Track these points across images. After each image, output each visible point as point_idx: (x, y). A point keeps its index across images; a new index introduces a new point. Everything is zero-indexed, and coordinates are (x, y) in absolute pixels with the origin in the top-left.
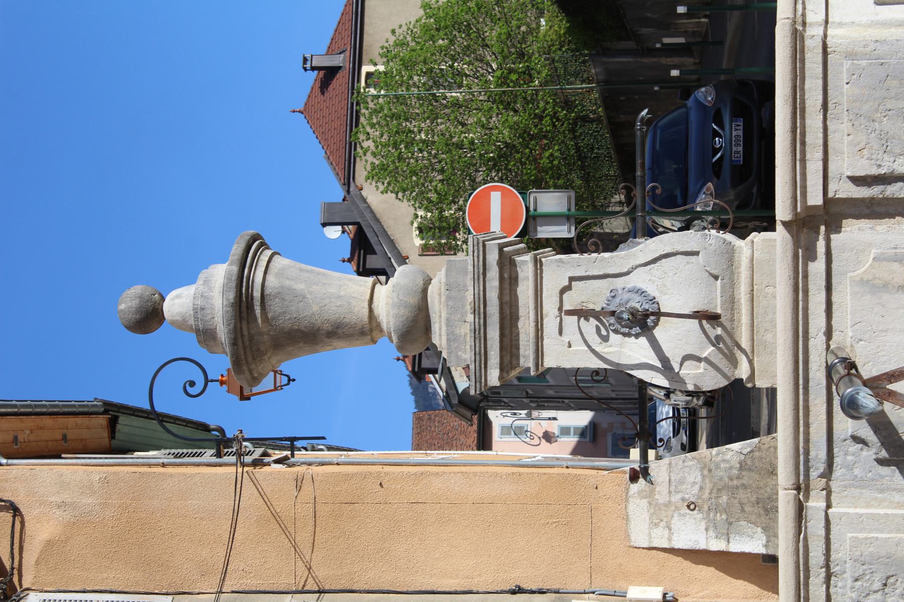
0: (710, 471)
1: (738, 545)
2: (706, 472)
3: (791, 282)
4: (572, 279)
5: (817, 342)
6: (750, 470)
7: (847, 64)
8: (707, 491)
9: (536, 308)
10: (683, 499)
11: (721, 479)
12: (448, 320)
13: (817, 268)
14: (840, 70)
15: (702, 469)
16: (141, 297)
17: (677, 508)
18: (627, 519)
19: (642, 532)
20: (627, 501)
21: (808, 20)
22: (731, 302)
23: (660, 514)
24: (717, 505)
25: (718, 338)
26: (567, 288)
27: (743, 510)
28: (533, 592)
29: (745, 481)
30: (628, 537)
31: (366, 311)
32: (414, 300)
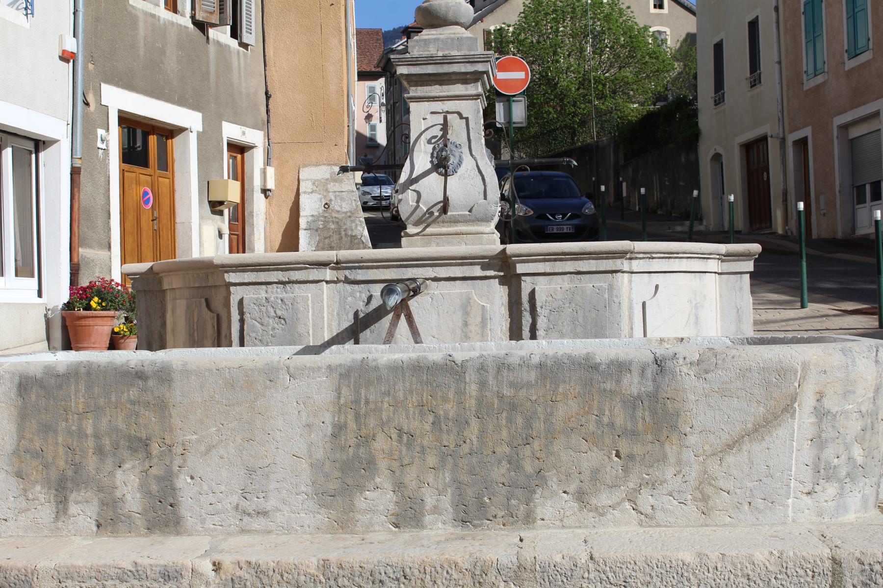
0: (350, 217)
2: (349, 214)
3: (468, 255)
4: (467, 119)
5: (430, 272)
6: (351, 242)
8: (336, 216)
9: (448, 97)
10: (331, 200)
11: (345, 224)
12: (438, 39)
13: (477, 271)
15: (350, 212)
17: (325, 197)
18: (317, 165)
19: (310, 175)
20: (328, 165)
21: (633, 261)
22: (455, 221)
23: (321, 186)
24: (328, 222)
25: (432, 213)
26: (461, 117)
27: (325, 238)
28: (267, 106)
29: (344, 239)
30: (305, 166)
32: (451, 16)
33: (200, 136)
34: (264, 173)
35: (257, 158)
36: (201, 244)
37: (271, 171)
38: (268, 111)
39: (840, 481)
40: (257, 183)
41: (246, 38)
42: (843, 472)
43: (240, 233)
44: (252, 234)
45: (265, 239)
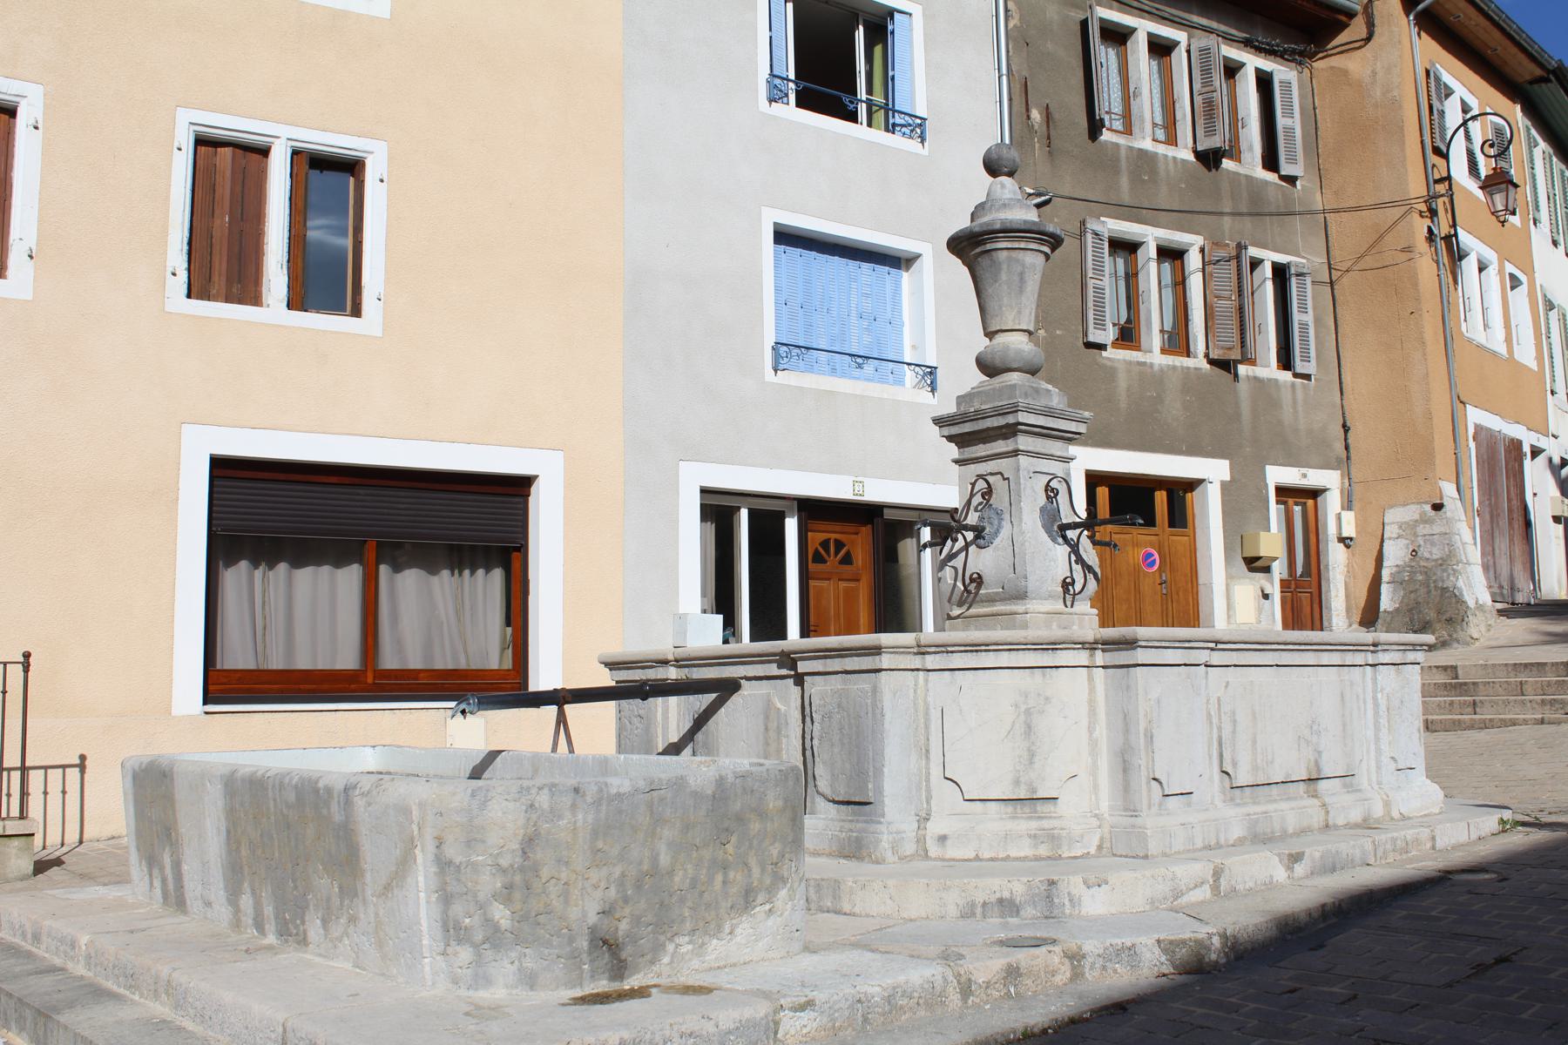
1: (1385, 590)
7: (867, 687)
14: (863, 683)
16: (1000, 158)
22: (991, 600)
23: (1409, 528)
25: (969, 592)
31: (993, 329)
32: (998, 363)
33: (1224, 485)
34: (1339, 517)
35: (1332, 503)
36: (1230, 606)
37: (1349, 518)
38: (1347, 448)
39: (475, 946)
40: (1332, 530)
41: (1300, 367)
42: (479, 937)
43: (1314, 590)
44: (1329, 591)
45: (1347, 596)
